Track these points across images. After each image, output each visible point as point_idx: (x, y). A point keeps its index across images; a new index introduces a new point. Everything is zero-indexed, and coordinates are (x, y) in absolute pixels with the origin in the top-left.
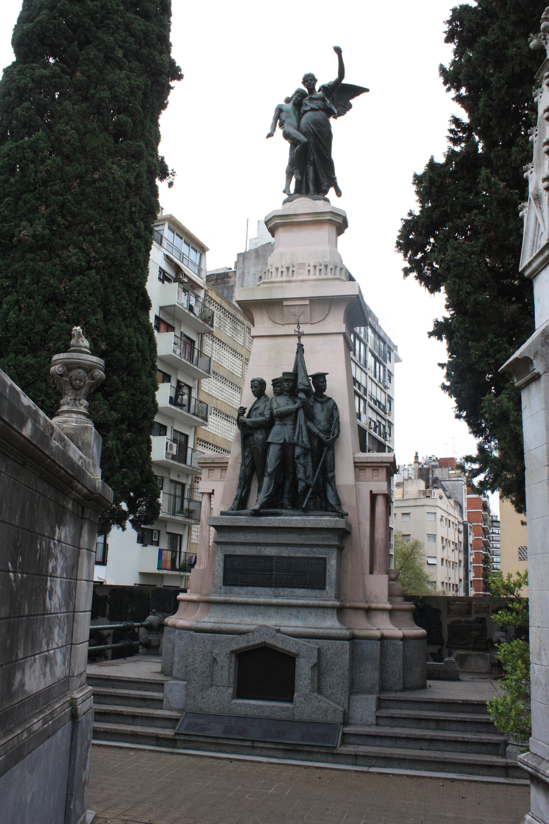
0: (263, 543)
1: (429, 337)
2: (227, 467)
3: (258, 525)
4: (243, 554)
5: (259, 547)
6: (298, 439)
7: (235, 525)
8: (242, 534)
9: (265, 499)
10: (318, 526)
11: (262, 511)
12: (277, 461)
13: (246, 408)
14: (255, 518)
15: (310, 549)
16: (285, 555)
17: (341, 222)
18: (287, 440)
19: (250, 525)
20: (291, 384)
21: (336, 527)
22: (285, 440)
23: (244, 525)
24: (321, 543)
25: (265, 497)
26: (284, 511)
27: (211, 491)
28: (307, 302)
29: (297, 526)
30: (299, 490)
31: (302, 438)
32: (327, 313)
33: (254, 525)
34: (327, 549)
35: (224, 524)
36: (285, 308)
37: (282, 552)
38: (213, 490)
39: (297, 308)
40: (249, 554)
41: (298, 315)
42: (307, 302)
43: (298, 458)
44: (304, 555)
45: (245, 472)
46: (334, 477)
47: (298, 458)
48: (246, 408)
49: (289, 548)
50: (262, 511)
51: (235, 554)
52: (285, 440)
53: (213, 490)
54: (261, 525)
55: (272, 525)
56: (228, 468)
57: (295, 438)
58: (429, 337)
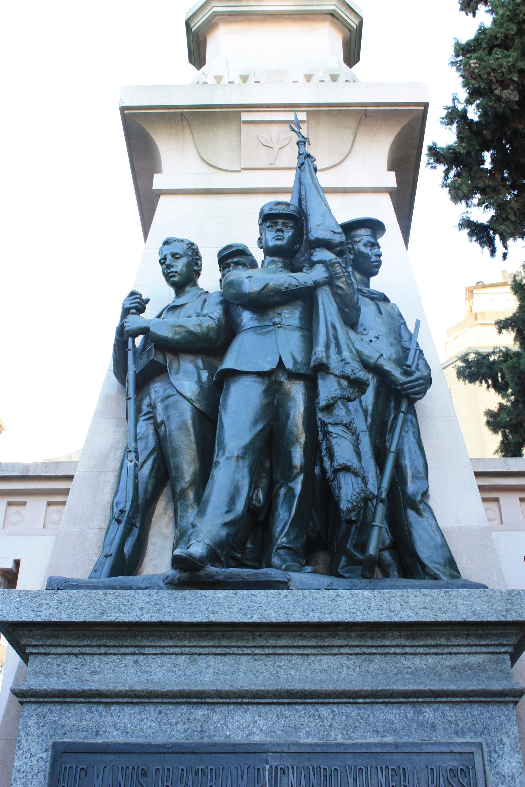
0: (219, 694)
1: (500, 332)
2: (66, 492)
3: (199, 618)
4: (132, 740)
5: (200, 712)
6: (328, 357)
7: (105, 619)
8: (130, 659)
9: (223, 533)
10: (443, 618)
11: (212, 569)
12: (255, 422)
13: (147, 301)
14: (187, 593)
15: (409, 712)
16: (310, 740)
17: (355, 27)
18: (289, 365)
19: (168, 618)
20: (288, 234)
21: (512, 617)
22: (281, 363)
23: (146, 618)
24: (452, 687)
25: (226, 525)
26: (295, 576)
27: (9, 565)
28: (302, 116)
29: (359, 618)
30: (344, 505)
31: (339, 352)
32: (347, 151)
33: (186, 619)
34: (477, 710)
35: (64, 617)
36: (244, 127)
37: (297, 730)
38: (17, 563)
39: (275, 128)
40: (160, 740)
41: (276, 147)
42: (302, 116)
43: (329, 408)
44: (389, 739)
45: (136, 477)
46: (425, 494)
47: (329, 408)
48: (147, 301)
49: (324, 711)
50: (212, 569)
51: (99, 740)
52: (281, 363)
53: (17, 563)
54: (213, 618)
55: (256, 618)
56: (70, 499)
57: (320, 350)
58: (500, 332)
